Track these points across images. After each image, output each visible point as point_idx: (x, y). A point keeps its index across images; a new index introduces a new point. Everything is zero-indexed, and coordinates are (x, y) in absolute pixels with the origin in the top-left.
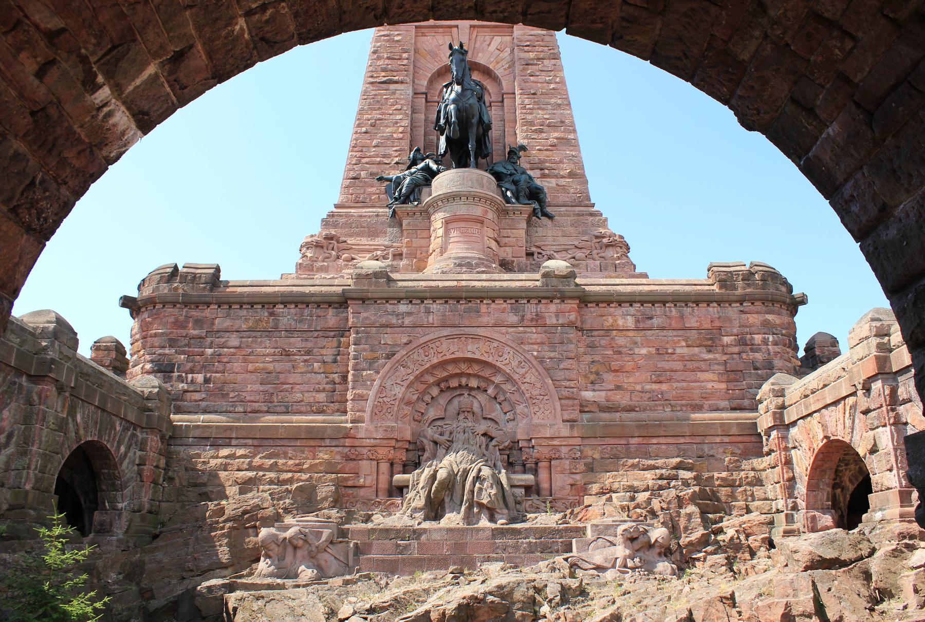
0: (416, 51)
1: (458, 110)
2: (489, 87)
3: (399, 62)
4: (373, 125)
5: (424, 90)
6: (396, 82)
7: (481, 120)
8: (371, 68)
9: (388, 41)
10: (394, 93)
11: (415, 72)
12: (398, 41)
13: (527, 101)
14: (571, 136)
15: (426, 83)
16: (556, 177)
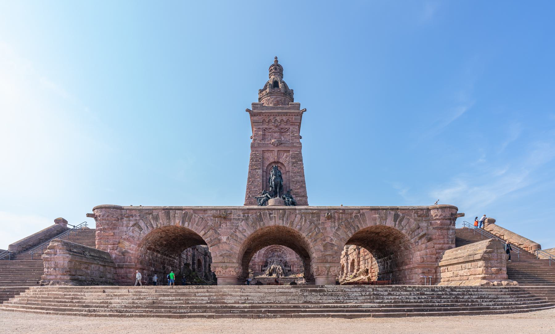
0: (263, 158)
1: (275, 183)
2: (283, 169)
3: (258, 162)
4: (252, 182)
5: (265, 170)
6: (258, 169)
7: (280, 184)
8: (251, 164)
9: (255, 155)
10: (257, 172)
11: (263, 165)
12: (258, 155)
13: (293, 175)
14: (304, 185)
15: (265, 168)
16: (299, 197)
